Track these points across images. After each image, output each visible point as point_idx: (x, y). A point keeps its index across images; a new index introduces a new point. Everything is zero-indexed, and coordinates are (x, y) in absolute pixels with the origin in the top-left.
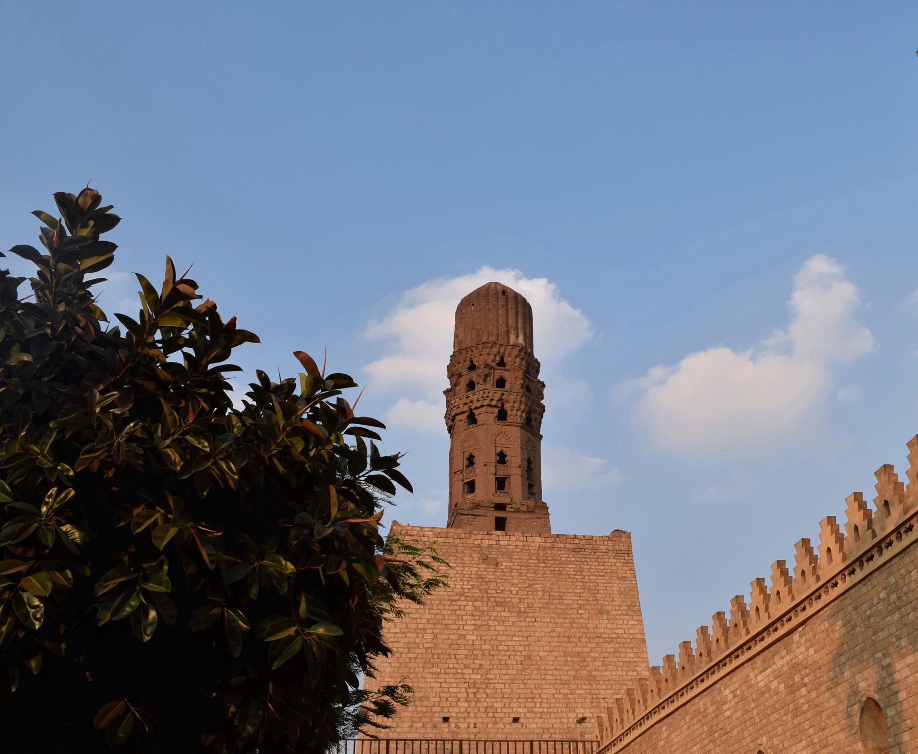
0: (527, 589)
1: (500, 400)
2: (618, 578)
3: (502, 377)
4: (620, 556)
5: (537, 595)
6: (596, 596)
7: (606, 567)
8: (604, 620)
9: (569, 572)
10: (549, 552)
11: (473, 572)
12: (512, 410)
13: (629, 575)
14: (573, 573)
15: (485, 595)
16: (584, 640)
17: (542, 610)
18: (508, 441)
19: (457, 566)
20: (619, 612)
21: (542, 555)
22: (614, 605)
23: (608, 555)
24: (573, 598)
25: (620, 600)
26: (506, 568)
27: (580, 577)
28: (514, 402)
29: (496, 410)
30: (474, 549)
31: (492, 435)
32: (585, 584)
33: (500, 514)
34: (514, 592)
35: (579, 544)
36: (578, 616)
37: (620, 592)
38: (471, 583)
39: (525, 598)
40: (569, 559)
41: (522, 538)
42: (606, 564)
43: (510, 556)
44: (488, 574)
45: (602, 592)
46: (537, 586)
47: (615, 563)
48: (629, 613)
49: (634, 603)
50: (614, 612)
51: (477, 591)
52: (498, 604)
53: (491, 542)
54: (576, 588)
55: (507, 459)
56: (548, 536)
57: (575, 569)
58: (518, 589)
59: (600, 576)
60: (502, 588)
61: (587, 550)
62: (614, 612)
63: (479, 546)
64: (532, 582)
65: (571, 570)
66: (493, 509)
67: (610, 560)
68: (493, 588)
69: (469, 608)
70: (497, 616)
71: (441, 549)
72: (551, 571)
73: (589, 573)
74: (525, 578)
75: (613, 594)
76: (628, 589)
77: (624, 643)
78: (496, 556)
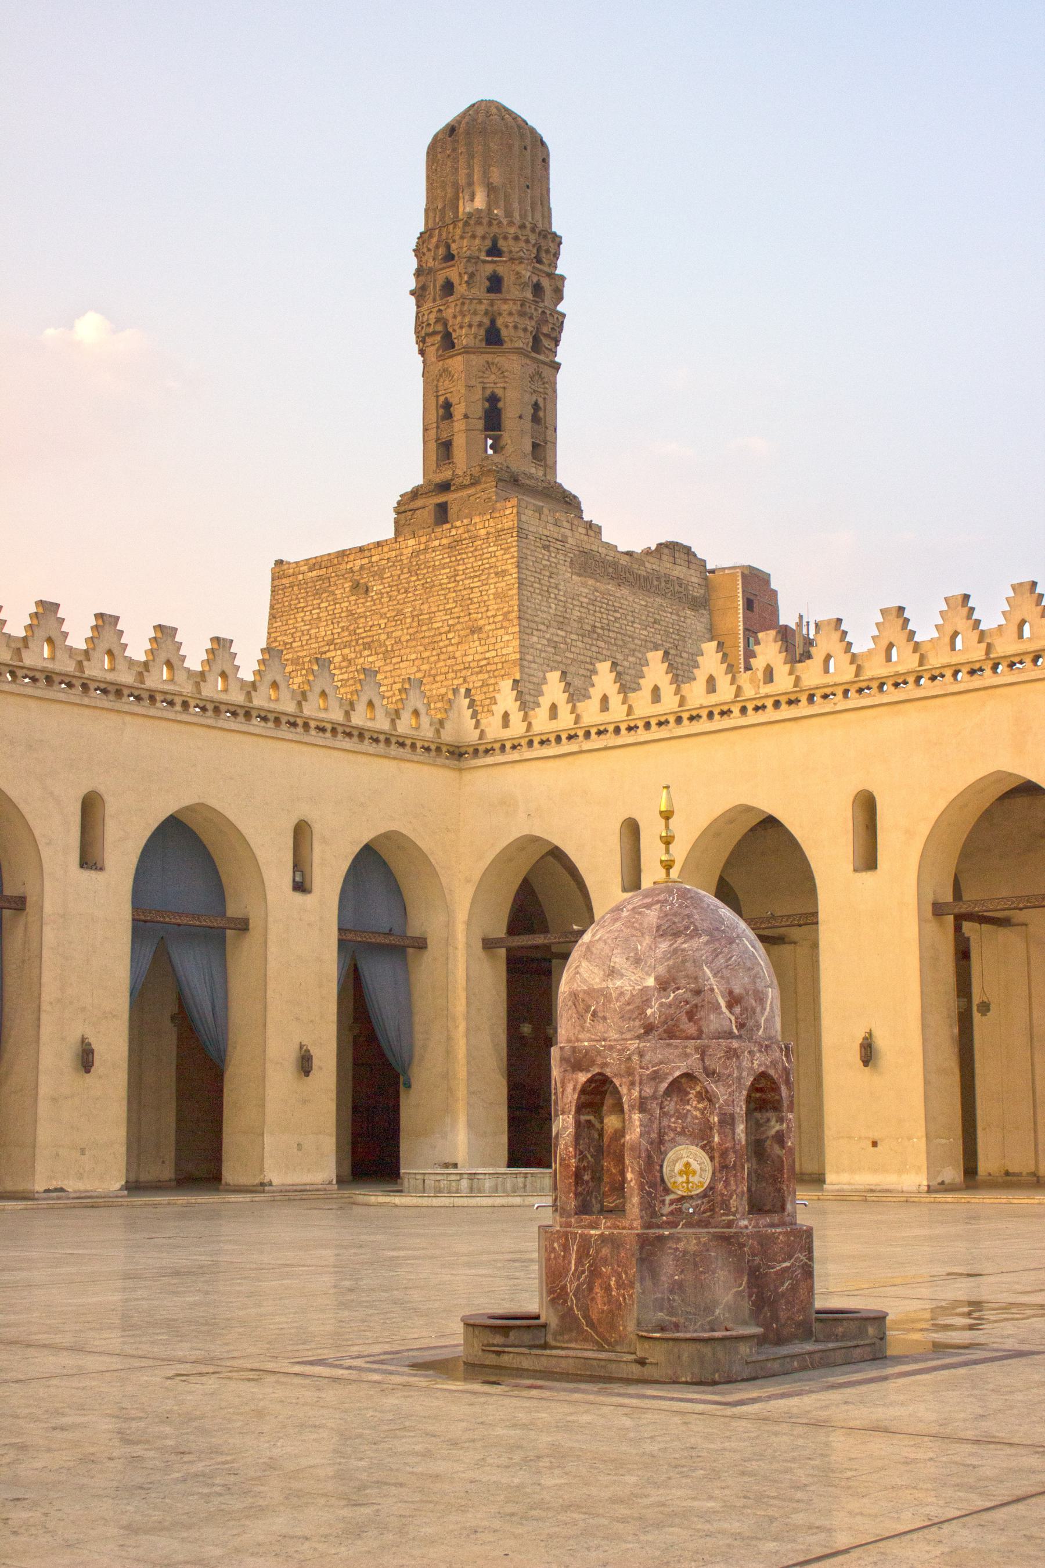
0: (396, 618)
1: (438, 320)
2: (496, 574)
3: (447, 278)
4: (502, 540)
5: (405, 623)
6: (469, 609)
8: (474, 641)
10: (422, 557)
11: (345, 609)
13: (510, 567)
14: (446, 581)
15: (353, 638)
16: (451, 675)
17: (410, 644)
19: (329, 605)
20: (493, 627)
21: (414, 563)
22: (487, 617)
23: (487, 542)
24: (444, 618)
25: (496, 607)
26: (376, 594)
28: (455, 317)
29: (438, 338)
30: (346, 576)
32: (458, 593)
33: (441, 499)
34: (383, 626)
36: (447, 642)
38: (340, 625)
39: (392, 632)
40: (443, 561)
41: (394, 545)
42: (486, 556)
43: (379, 575)
44: (358, 608)
45: (475, 600)
46: (406, 610)
47: (495, 552)
48: (504, 624)
50: (487, 628)
51: (346, 633)
52: (367, 646)
53: (365, 561)
54: (448, 603)
56: (421, 534)
58: (386, 621)
59: (476, 576)
60: (370, 623)
61: (464, 542)
62: (487, 628)
63: (351, 570)
64: (401, 607)
65: (445, 577)
67: (490, 549)
68: (361, 625)
69: (337, 659)
70: (363, 663)
71: (315, 586)
72: (423, 584)
73: (463, 577)
74: (395, 602)
75: (489, 600)
76: (508, 587)
77: (494, 671)
78: (366, 580)
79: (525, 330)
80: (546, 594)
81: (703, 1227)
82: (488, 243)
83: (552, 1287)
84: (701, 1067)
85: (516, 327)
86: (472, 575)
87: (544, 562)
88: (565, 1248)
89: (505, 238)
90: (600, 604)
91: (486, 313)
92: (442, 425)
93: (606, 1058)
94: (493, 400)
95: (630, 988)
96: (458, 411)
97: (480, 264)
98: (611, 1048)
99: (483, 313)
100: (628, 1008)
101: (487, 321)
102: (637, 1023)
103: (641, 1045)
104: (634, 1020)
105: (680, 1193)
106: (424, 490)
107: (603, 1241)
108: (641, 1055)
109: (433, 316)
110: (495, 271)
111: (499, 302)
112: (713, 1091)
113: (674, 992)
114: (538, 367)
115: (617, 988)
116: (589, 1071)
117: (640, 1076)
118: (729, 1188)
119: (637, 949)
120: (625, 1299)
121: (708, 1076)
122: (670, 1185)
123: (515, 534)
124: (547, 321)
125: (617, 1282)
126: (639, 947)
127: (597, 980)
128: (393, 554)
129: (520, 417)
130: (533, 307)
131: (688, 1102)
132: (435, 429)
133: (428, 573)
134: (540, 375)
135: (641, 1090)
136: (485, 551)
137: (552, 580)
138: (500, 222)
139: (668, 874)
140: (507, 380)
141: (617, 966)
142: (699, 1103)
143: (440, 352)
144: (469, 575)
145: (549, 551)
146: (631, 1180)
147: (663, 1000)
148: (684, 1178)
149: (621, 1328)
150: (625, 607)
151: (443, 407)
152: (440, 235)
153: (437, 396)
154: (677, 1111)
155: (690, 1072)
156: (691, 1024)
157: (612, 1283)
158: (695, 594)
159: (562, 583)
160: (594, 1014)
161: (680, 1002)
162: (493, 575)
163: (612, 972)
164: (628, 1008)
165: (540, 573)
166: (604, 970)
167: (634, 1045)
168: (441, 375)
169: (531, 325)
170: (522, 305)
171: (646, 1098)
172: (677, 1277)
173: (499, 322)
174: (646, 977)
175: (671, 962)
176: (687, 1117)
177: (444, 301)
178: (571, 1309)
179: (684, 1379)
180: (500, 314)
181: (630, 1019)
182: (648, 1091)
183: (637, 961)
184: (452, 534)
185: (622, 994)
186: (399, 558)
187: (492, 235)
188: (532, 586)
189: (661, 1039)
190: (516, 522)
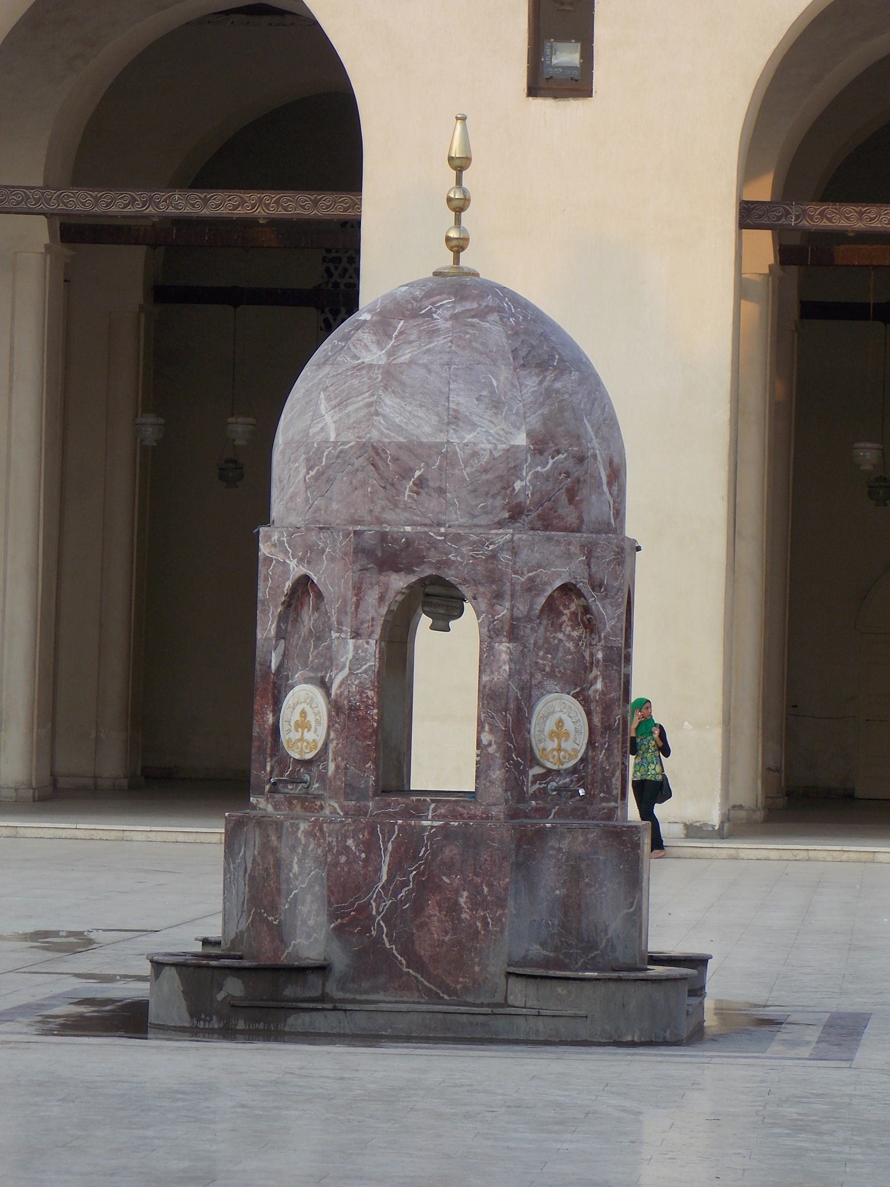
81: (578, 818)
83: (337, 909)
84: (586, 575)
88: (371, 847)
93: (447, 554)
95: (489, 446)
98: (458, 538)
100: (485, 477)
102: (499, 502)
103: (517, 537)
104: (494, 496)
105: (549, 765)
107: (446, 837)
108: (515, 553)
112: (598, 611)
113: (553, 458)
115: (466, 445)
116: (414, 572)
117: (512, 585)
118: (611, 760)
119: (491, 384)
120: (486, 924)
121: (593, 589)
122: (538, 753)
125: (471, 899)
126: (495, 383)
127: (427, 429)
131: (559, 628)
135: (513, 607)
139: (457, 260)
141: (462, 409)
142: (573, 629)
146: (490, 745)
147: (539, 469)
148: (555, 745)
149: (477, 969)
154: (546, 640)
155: (573, 581)
156: (572, 507)
157: (462, 901)
160: (421, 483)
161: (560, 474)
163: (455, 419)
164: (485, 477)
166: (438, 414)
167: (503, 535)
171: (518, 619)
172: (557, 892)
174: (513, 430)
175: (546, 410)
176: (558, 650)
178: (379, 940)
179: (629, 1038)
181: (487, 494)
182: (522, 608)
183: (496, 405)
185: (475, 454)
189: (532, 529)
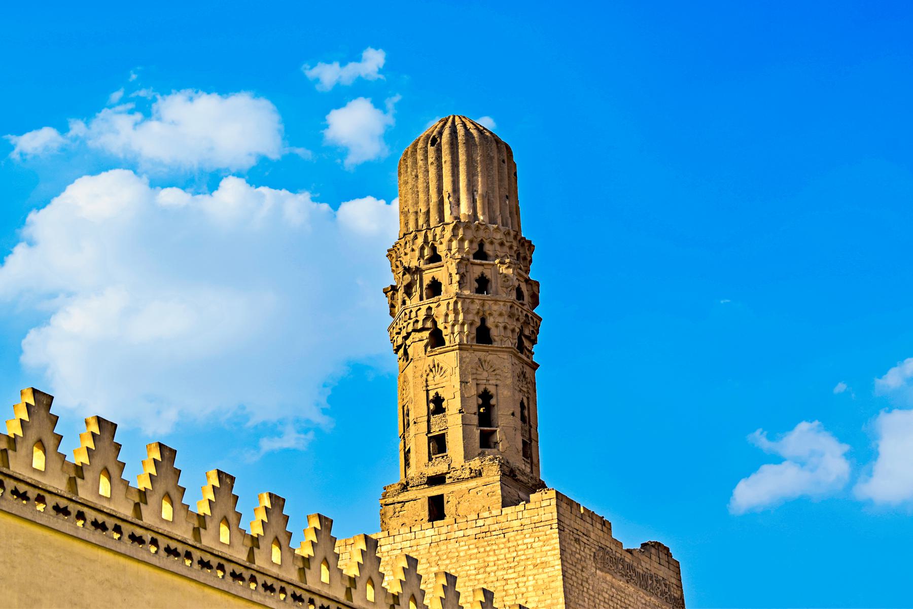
1: (429, 317)
2: (535, 566)
3: (433, 278)
7: (520, 553)
9: (469, 572)
10: (444, 547)
12: (446, 328)
13: (551, 559)
18: (443, 376)
21: (434, 554)
25: (537, 599)
27: (484, 575)
29: (426, 334)
31: (422, 376)
33: (435, 491)
35: (484, 525)
37: (536, 588)
40: (470, 552)
42: (520, 547)
49: (556, 601)
55: (444, 404)
57: (477, 566)
61: (494, 533)
65: (472, 568)
66: (426, 486)
67: (526, 541)
73: (495, 568)
75: (528, 592)
76: (551, 579)
79: (513, 331)
80: (581, 587)
82: (476, 247)
85: (505, 328)
86: (506, 566)
87: (577, 556)
89: (492, 243)
90: (616, 600)
91: (478, 313)
92: (432, 419)
94: (485, 397)
96: (453, 404)
97: (469, 266)
99: (475, 312)
101: (478, 323)
106: (416, 482)
109: (422, 314)
110: (482, 274)
111: (491, 302)
114: (523, 367)
123: (555, 526)
124: (529, 324)
128: (408, 544)
129: (513, 414)
130: (520, 309)
132: (426, 423)
133: (451, 563)
134: (524, 376)
136: (520, 542)
137: (584, 574)
138: (487, 228)
140: (498, 377)
143: (429, 349)
144: (500, 567)
145: (579, 544)
150: (632, 604)
151: (433, 401)
152: (426, 237)
153: (428, 391)
158: (675, 595)
159: (590, 577)
162: (531, 567)
165: (575, 566)
168: (431, 370)
169: (517, 326)
170: (511, 307)
173: (490, 322)
177: (432, 300)
180: (490, 314)
184: (477, 525)
186: (415, 548)
187: (480, 239)
188: (571, 579)
190: (555, 515)
